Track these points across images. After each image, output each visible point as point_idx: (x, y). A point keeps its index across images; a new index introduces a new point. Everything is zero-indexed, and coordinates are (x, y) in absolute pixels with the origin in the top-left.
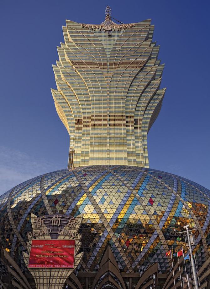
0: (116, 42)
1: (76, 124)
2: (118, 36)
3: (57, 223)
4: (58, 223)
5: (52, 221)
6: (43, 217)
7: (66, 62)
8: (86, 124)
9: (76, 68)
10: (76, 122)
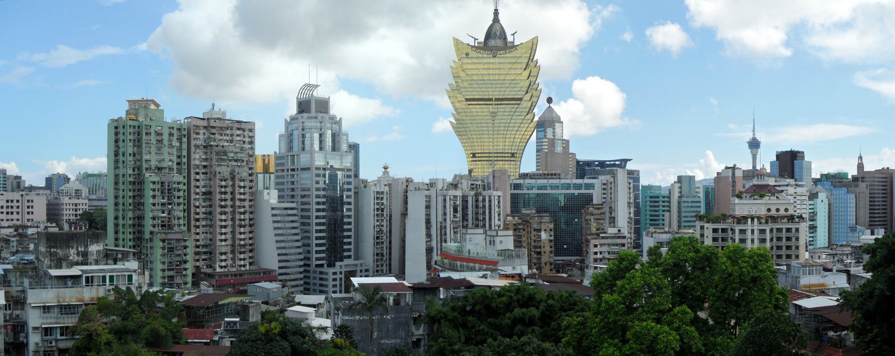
1: (472, 157)
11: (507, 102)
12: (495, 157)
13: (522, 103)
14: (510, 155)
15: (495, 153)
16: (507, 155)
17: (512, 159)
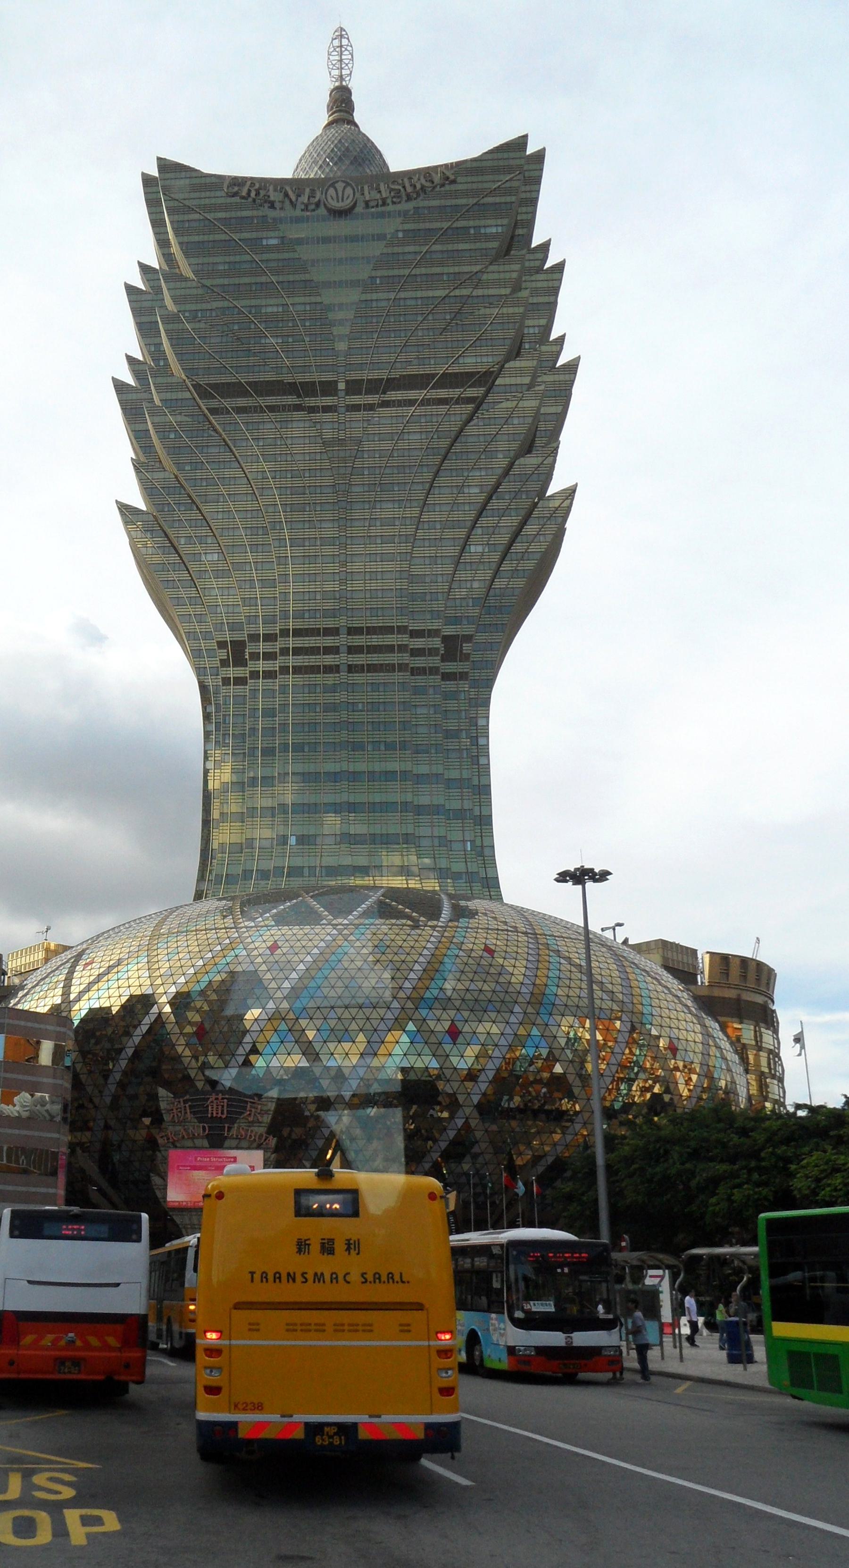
0: (374, 274)
1: (224, 663)
2: (381, 237)
4: (222, 1113)
5: (208, 1106)
6: (187, 1097)
7: (169, 380)
8: (261, 666)
9: (214, 411)
10: (222, 654)
11: (412, 394)
12: (351, 650)
13: (490, 399)
14: (436, 643)
15: (352, 631)
16: (418, 643)
17: (451, 667)
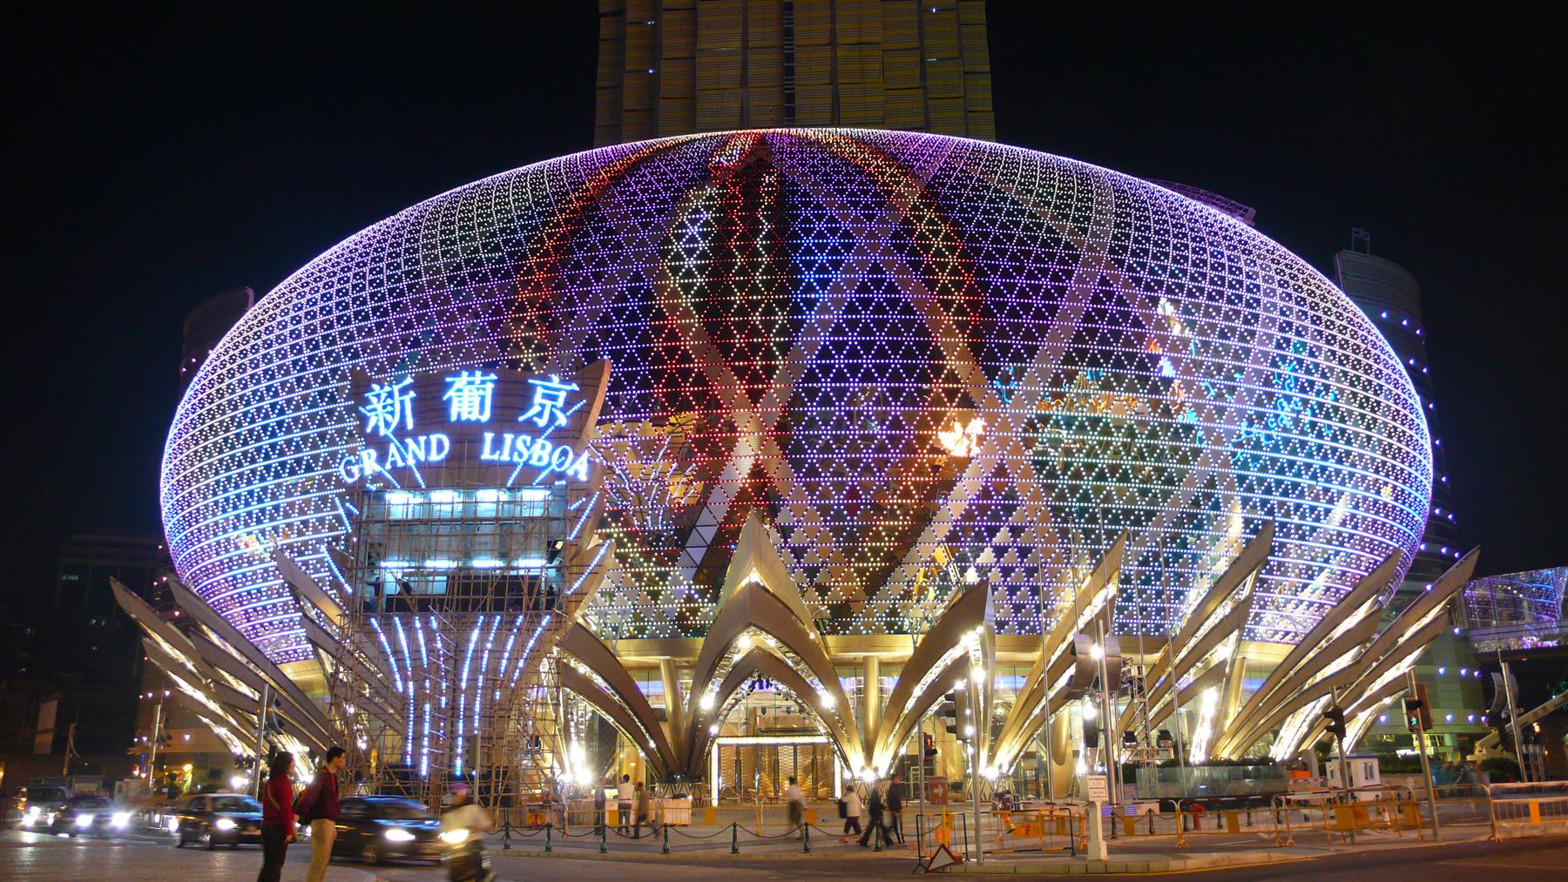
3: (476, 409)
4: (482, 412)
